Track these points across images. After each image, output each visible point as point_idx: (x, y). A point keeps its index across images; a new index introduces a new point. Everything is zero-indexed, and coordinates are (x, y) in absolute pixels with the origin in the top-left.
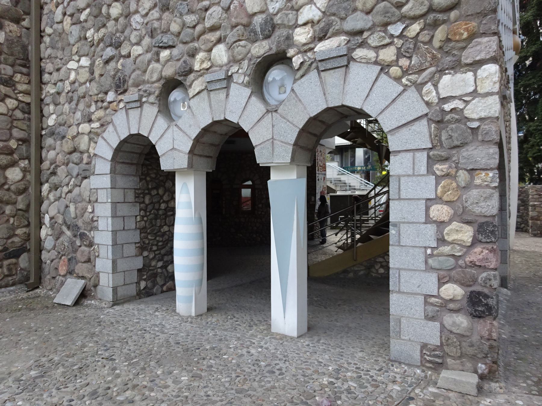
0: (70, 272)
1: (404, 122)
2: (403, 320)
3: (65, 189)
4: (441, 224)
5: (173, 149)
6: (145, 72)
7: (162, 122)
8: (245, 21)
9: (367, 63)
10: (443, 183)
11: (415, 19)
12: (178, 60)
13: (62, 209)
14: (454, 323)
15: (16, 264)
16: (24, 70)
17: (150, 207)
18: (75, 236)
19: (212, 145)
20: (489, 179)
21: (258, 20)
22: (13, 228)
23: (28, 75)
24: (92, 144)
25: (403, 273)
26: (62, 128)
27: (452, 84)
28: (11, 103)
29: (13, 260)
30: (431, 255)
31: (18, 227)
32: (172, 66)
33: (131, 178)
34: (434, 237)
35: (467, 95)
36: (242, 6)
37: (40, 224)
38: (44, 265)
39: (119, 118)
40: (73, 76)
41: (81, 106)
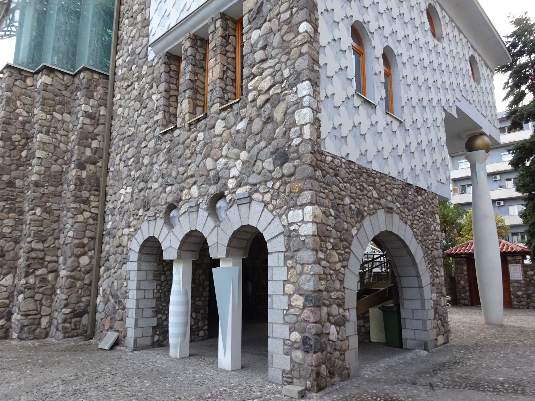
0: (111, 328)
1: (274, 236)
2: (274, 355)
3: (113, 271)
4: (290, 296)
5: (170, 247)
6: (159, 198)
7: (165, 230)
8: (206, 173)
9: (259, 201)
10: (291, 271)
11: (278, 179)
12: (175, 193)
13: (110, 284)
14: (296, 356)
15: (80, 321)
16: (96, 193)
17: (164, 283)
18: (116, 303)
19: (195, 243)
20: (309, 270)
21: (212, 173)
22: (80, 297)
23: (98, 196)
24: (129, 242)
25: (274, 325)
26: (115, 230)
27: (294, 215)
28: (87, 214)
29: (78, 319)
30: (286, 315)
31: (84, 296)
32: (171, 196)
33: (152, 264)
34: (287, 304)
35: (299, 222)
36: (204, 165)
37: (97, 294)
38: (97, 323)
39: (144, 226)
41: (125, 217)
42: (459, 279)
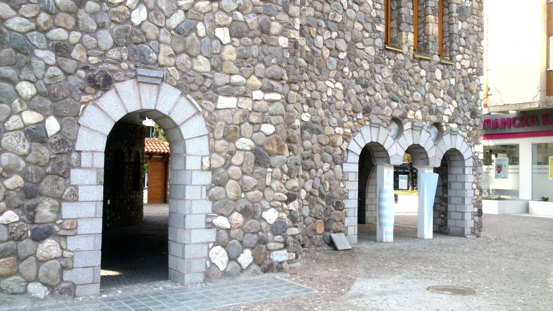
4: (474, 190)
5: (397, 154)
39: (366, 130)
40: (330, 93)
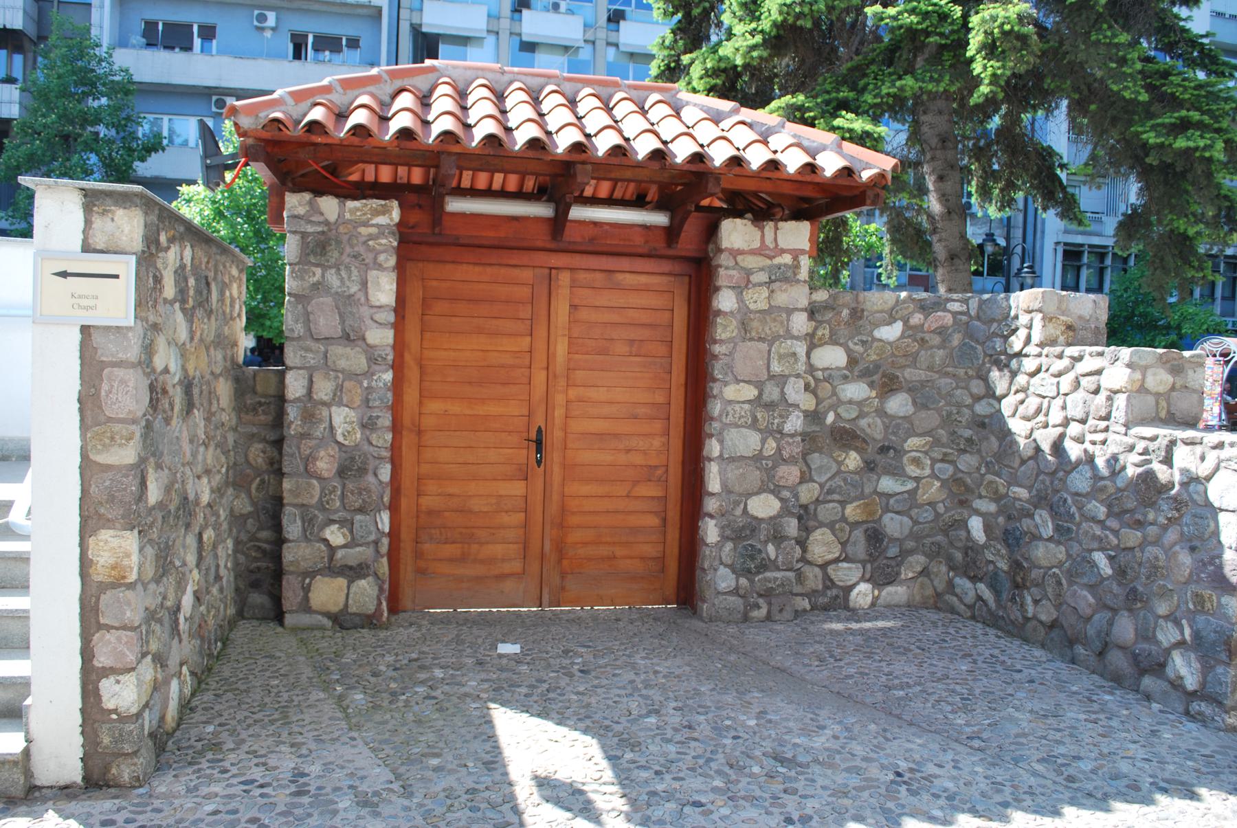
42: (324, 389)
